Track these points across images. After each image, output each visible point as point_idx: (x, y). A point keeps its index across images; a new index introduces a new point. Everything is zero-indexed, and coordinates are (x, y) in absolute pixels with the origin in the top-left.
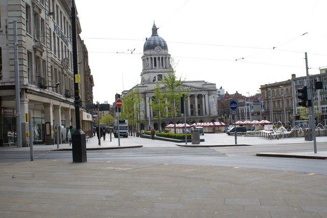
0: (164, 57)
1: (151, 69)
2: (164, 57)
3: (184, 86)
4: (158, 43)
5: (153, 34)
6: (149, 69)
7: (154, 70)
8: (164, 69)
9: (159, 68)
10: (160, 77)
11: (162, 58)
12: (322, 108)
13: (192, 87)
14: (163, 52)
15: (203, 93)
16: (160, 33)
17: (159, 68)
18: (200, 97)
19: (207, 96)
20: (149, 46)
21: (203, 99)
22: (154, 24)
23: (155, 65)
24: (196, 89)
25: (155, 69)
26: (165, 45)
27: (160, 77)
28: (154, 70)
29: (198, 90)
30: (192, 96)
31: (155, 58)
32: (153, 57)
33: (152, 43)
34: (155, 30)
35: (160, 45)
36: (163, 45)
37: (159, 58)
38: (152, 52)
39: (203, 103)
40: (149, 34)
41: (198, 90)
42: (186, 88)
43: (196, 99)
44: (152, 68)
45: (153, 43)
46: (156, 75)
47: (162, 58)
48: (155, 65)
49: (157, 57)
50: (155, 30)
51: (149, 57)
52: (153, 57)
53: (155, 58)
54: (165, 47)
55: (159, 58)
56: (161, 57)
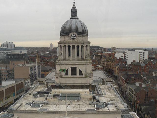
0: (80, 45)
2: (80, 45)
4: (74, 27)
5: (71, 16)
6: (62, 60)
7: (66, 62)
8: (78, 60)
9: (74, 59)
10: (74, 70)
11: (78, 47)
14: (81, 39)
20: (65, 32)
22: (74, 5)
23: (69, 55)
25: (69, 60)
27: (74, 70)
28: (66, 62)
31: (69, 47)
32: (67, 45)
34: (74, 11)
35: (76, 31)
36: (80, 30)
37: (74, 47)
38: (67, 39)
44: (65, 59)
46: (69, 68)
47: (78, 47)
48: (69, 55)
50: (74, 11)
51: (62, 45)
52: (67, 45)
53: (69, 47)
54: (84, 33)
55: (74, 47)
56: (76, 45)
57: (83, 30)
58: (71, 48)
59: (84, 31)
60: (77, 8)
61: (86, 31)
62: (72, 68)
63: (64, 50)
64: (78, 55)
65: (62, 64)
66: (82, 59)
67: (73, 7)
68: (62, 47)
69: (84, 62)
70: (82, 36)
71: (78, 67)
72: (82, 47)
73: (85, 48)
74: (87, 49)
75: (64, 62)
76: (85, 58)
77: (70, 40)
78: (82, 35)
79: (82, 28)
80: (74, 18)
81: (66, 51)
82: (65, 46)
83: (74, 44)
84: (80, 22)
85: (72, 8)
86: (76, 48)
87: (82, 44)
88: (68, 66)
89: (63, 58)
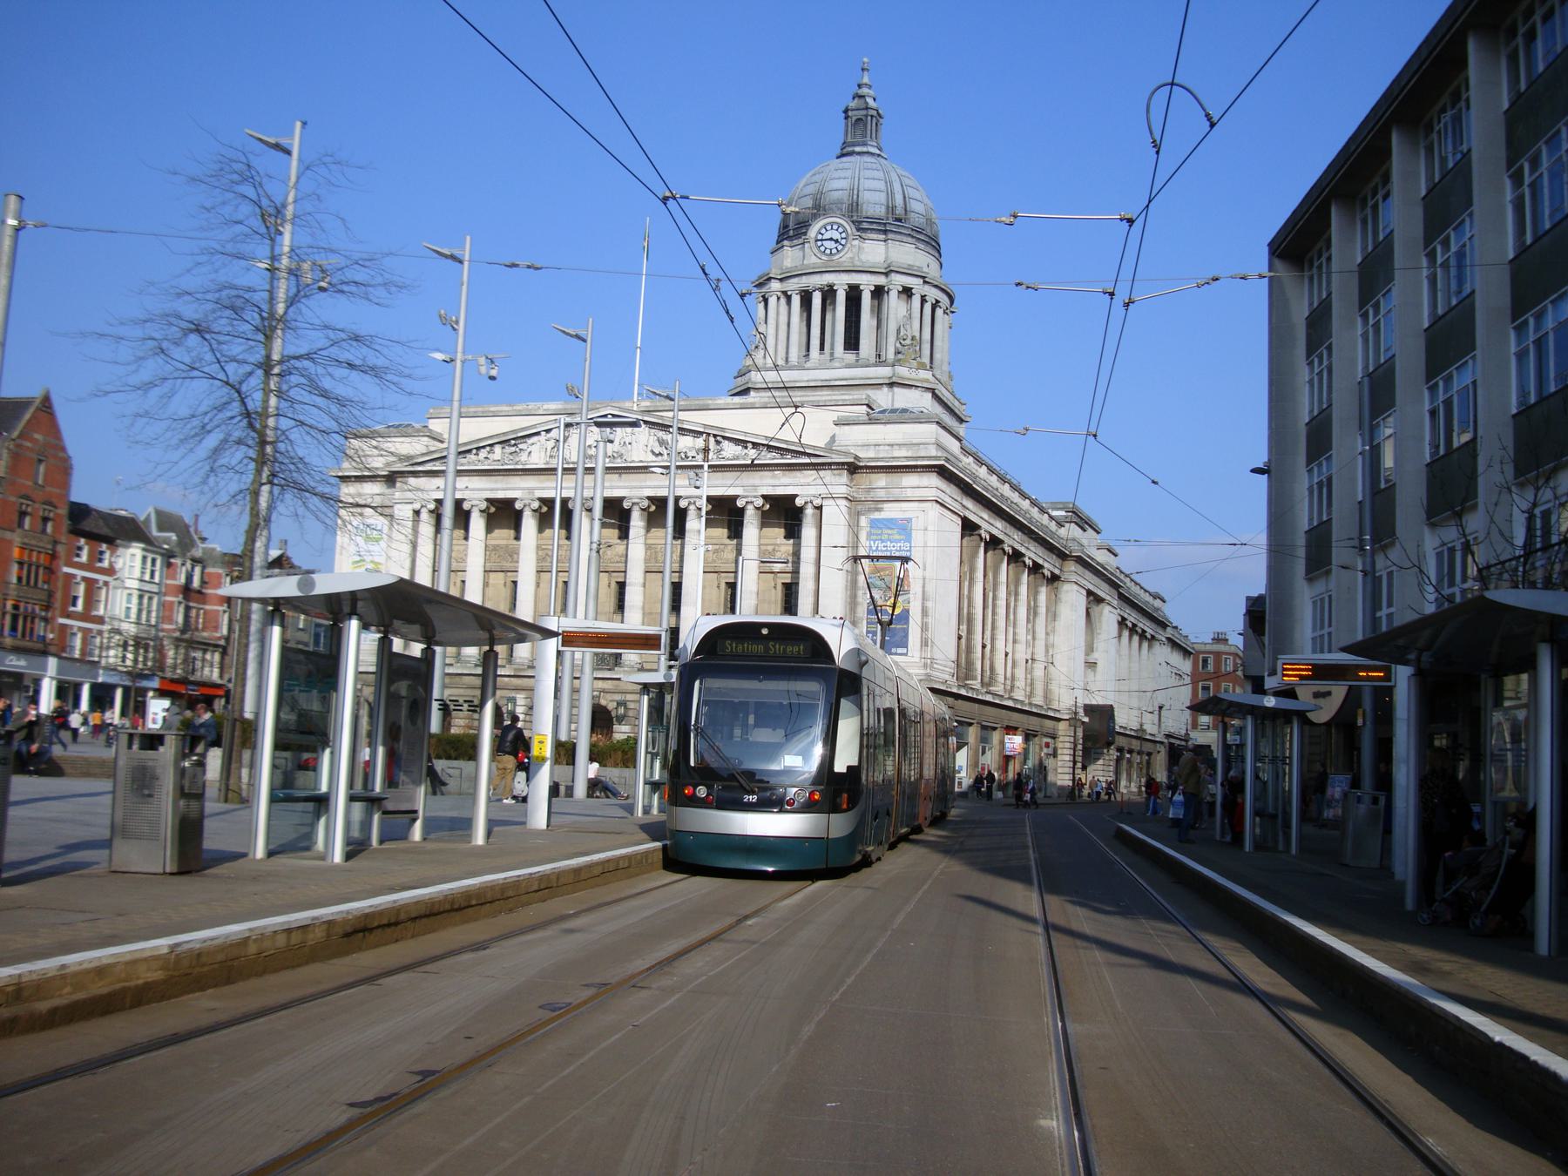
0: (867, 283)
2: (867, 283)
7: (787, 376)
8: (857, 364)
11: (854, 294)
14: (874, 251)
19: (835, 515)
21: (808, 532)
25: (800, 368)
29: (768, 458)
36: (874, 203)
41: (768, 458)
45: (809, 203)
47: (854, 294)
55: (829, 294)
56: (841, 282)
57: (891, 209)
58: (817, 299)
59: (899, 211)
64: (852, 342)
68: (772, 301)
69: (884, 372)
70: (882, 237)
72: (879, 292)
73: (894, 302)
77: (814, 260)
78: (885, 232)
80: (858, 149)
86: (841, 297)
87: (881, 280)
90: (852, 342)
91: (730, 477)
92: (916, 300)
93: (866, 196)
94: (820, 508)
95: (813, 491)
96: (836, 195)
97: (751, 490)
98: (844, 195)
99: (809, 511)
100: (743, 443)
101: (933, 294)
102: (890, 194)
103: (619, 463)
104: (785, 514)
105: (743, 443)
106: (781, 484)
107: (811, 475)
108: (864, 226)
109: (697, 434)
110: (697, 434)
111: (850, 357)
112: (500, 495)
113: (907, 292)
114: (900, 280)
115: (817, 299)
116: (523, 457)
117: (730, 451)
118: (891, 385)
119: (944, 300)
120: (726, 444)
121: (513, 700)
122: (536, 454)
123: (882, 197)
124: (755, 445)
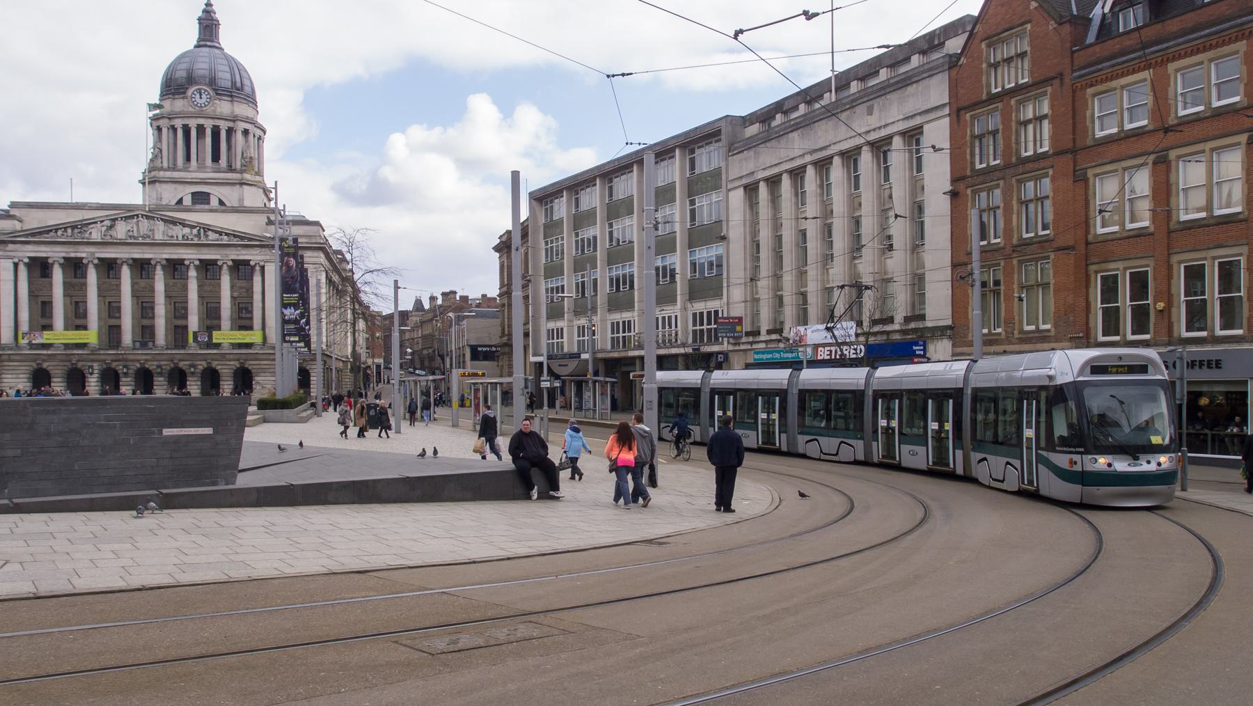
0: (224, 126)
1: (169, 169)
3: (174, 222)
5: (200, 40)
6: (162, 169)
7: (176, 175)
9: (202, 167)
11: (216, 132)
12: (615, 327)
13: (206, 229)
14: (224, 107)
15: (254, 256)
16: (228, 40)
17: (202, 167)
18: (242, 270)
20: (174, 86)
21: (257, 279)
23: (188, 158)
24: (225, 240)
25: (185, 169)
26: (234, 83)
28: (176, 175)
30: (208, 268)
31: (187, 130)
32: (178, 123)
33: (181, 74)
34: (208, 26)
35: (212, 82)
36: (224, 78)
37: (201, 129)
38: (179, 105)
39: (257, 297)
40: (189, 37)
42: (179, 231)
43: (226, 280)
45: (184, 74)
46: (186, 193)
47: (216, 132)
48: (188, 158)
49: (193, 123)
50: (208, 26)
52: (178, 123)
53: (187, 130)
55: (201, 129)
56: (208, 124)
57: (234, 83)
58: (194, 133)
59: (239, 85)
60: (218, 16)
61: (247, 89)
62: (193, 194)
63: (171, 141)
65: (160, 182)
66: (230, 169)
67: (204, 11)
68: (165, 131)
71: (216, 192)
72: (230, 131)
73: (239, 138)
74: (247, 141)
75: (168, 174)
76: (238, 166)
79: (233, 75)
81: (175, 144)
82: (174, 129)
83: (201, 121)
84: (228, 58)
85: (200, 14)
86: (209, 132)
87: (231, 124)
88: (180, 187)
89: (165, 165)
90: (216, 157)
91: (213, 250)
92: (251, 136)
93: (220, 75)
94: (263, 268)
95: (259, 258)
96: (201, 72)
97: (226, 257)
98: (206, 73)
99: (258, 268)
100: (220, 233)
101: (259, 132)
102: (233, 75)
103: (148, 241)
104: (242, 270)
105: (220, 233)
106: (244, 255)
107: (256, 251)
108: (219, 92)
109: (192, 227)
110: (192, 227)
111: (215, 165)
112: (73, 255)
113: (246, 132)
114: (242, 126)
115: (194, 133)
116: (87, 235)
117: (212, 236)
118: (242, 184)
119: (261, 133)
120: (210, 233)
121: (91, 367)
122: (96, 234)
123: (228, 76)
124: (227, 234)
